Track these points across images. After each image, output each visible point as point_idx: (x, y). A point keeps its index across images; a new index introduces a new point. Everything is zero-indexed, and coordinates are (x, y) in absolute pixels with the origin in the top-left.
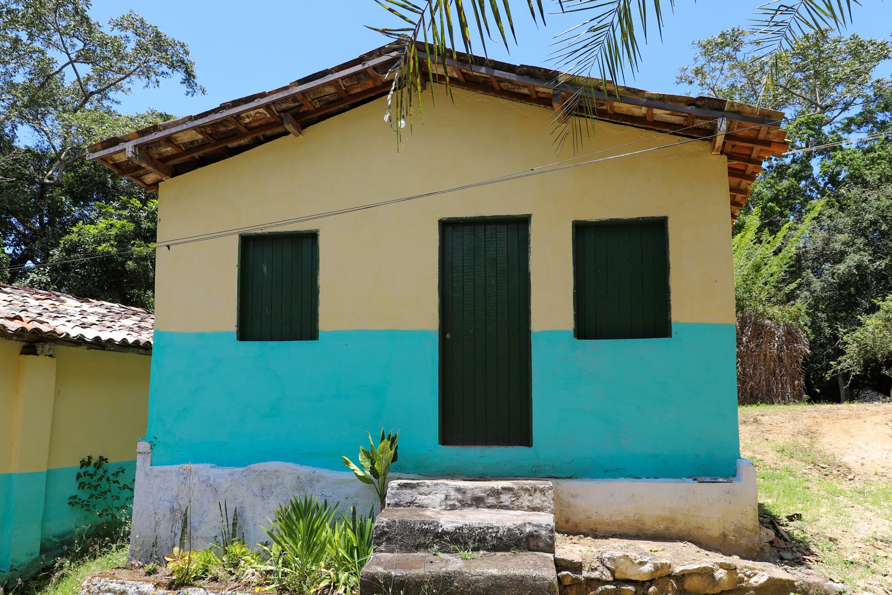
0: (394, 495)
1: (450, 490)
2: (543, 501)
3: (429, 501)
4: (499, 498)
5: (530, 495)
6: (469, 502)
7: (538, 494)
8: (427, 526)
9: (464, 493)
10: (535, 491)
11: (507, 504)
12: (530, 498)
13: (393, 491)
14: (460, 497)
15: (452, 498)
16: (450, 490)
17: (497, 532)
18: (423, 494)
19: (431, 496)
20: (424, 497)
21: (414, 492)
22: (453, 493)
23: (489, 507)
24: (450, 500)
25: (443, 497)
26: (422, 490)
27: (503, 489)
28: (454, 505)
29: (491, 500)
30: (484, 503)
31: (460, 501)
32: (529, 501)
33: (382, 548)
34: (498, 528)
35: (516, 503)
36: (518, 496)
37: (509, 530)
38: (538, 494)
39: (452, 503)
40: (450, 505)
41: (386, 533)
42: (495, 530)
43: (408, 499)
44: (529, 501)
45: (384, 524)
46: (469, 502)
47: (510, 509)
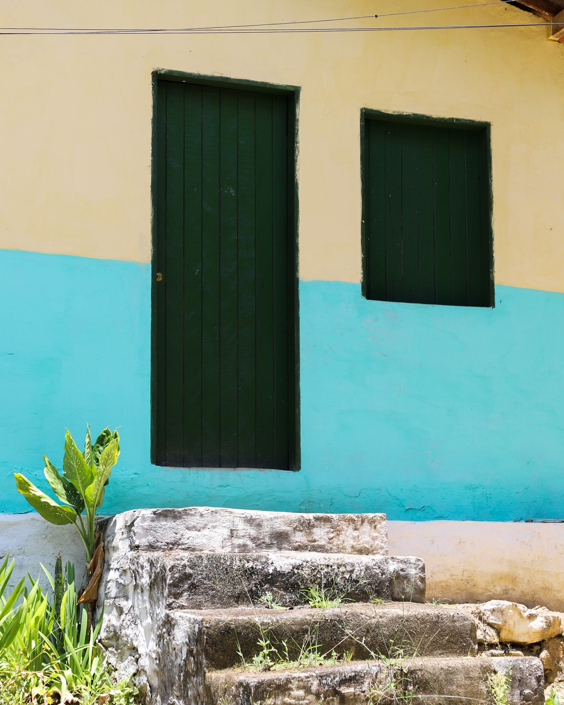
0: (147, 530)
1: (237, 520)
2: (374, 539)
3: (205, 541)
4: (310, 533)
5: (356, 529)
6: (267, 540)
7: (366, 527)
8: (250, 565)
9: (259, 525)
10: (363, 521)
11: (322, 543)
12: (356, 533)
13: (146, 524)
14: (253, 532)
15: (241, 533)
16: (237, 520)
17: (352, 572)
18: (194, 528)
19: (206, 532)
20: (194, 533)
21: (178, 525)
22: (241, 527)
23: (296, 549)
24: (238, 537)
25: (227, 532)
26: (192, 521)
27: (317, 519)
28: (245, 546)
29: (299, 538)
30: (289, 542)
31: (253, 539)
32: (354, 538)
33: (182, 601)
34: (353, 565)
35: (335, 541)
36: (338, 531)
37: (367, 568)
38: (366, 527)
39: (241, 541)
40: (239, 546)
41: (188, 577)
42: (349, 568)
43: (170, 537)
44: (354, 538)
45: (185, 562)
46: (267, 540)
47: (327, 551)
